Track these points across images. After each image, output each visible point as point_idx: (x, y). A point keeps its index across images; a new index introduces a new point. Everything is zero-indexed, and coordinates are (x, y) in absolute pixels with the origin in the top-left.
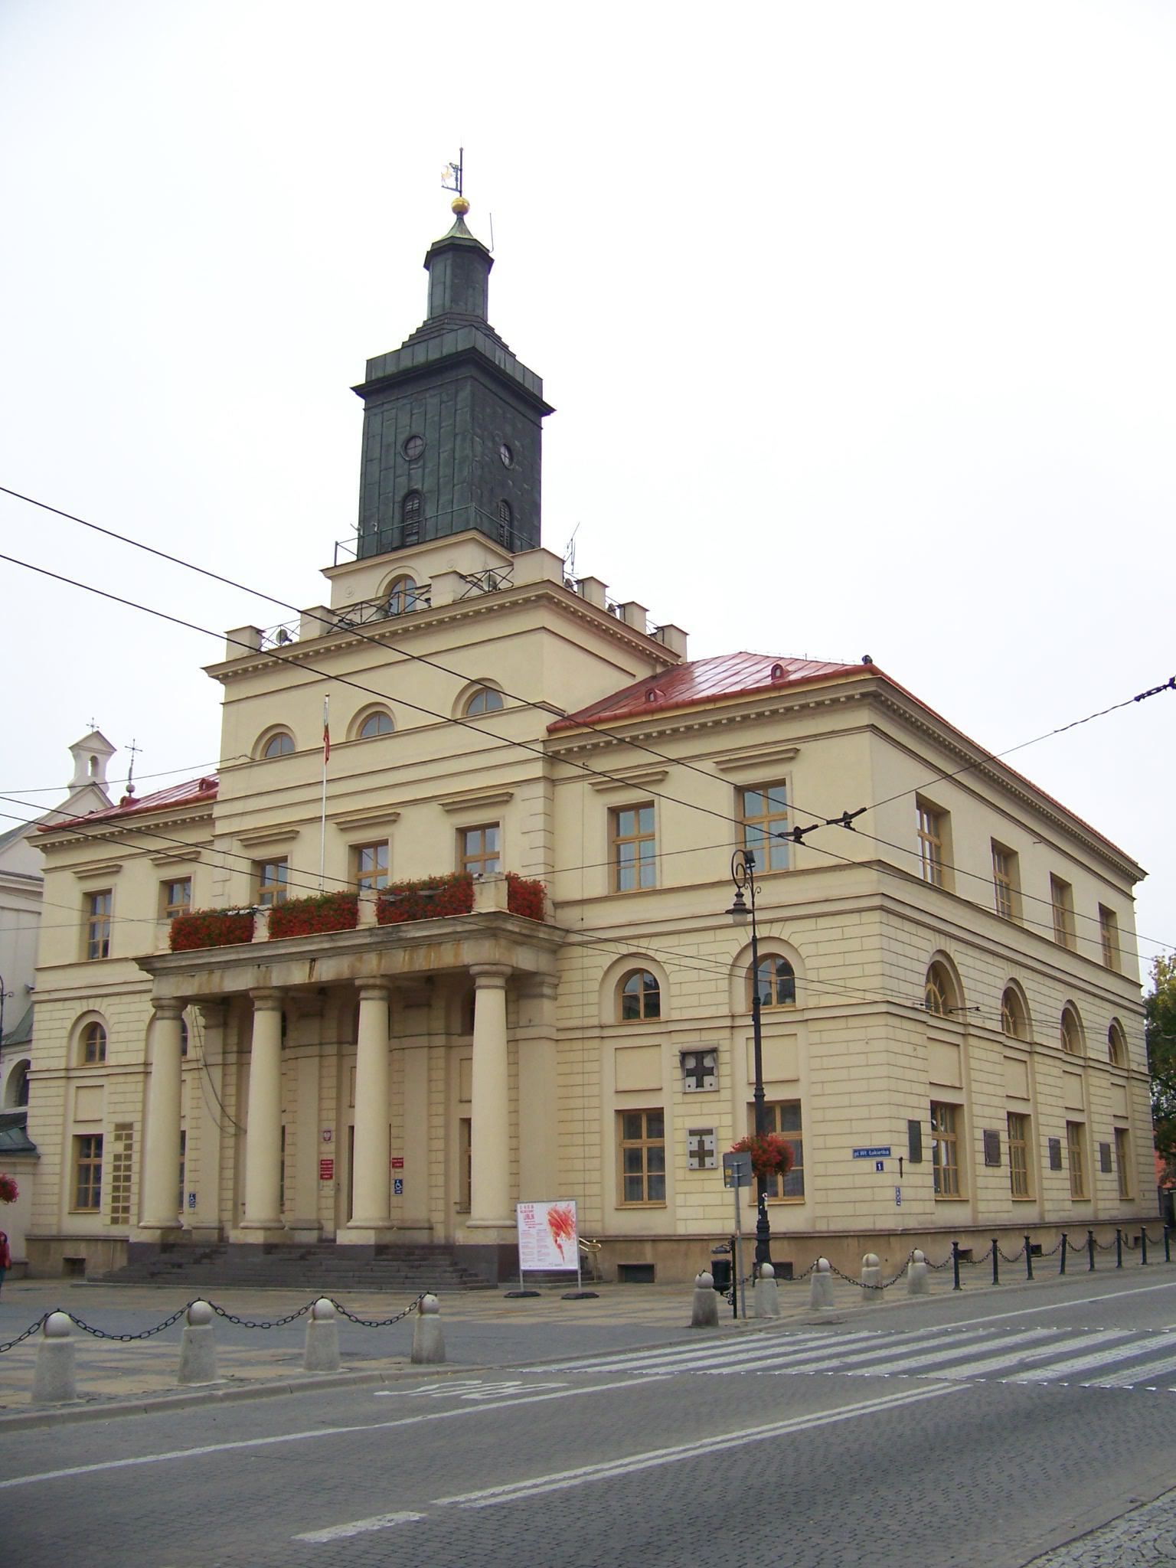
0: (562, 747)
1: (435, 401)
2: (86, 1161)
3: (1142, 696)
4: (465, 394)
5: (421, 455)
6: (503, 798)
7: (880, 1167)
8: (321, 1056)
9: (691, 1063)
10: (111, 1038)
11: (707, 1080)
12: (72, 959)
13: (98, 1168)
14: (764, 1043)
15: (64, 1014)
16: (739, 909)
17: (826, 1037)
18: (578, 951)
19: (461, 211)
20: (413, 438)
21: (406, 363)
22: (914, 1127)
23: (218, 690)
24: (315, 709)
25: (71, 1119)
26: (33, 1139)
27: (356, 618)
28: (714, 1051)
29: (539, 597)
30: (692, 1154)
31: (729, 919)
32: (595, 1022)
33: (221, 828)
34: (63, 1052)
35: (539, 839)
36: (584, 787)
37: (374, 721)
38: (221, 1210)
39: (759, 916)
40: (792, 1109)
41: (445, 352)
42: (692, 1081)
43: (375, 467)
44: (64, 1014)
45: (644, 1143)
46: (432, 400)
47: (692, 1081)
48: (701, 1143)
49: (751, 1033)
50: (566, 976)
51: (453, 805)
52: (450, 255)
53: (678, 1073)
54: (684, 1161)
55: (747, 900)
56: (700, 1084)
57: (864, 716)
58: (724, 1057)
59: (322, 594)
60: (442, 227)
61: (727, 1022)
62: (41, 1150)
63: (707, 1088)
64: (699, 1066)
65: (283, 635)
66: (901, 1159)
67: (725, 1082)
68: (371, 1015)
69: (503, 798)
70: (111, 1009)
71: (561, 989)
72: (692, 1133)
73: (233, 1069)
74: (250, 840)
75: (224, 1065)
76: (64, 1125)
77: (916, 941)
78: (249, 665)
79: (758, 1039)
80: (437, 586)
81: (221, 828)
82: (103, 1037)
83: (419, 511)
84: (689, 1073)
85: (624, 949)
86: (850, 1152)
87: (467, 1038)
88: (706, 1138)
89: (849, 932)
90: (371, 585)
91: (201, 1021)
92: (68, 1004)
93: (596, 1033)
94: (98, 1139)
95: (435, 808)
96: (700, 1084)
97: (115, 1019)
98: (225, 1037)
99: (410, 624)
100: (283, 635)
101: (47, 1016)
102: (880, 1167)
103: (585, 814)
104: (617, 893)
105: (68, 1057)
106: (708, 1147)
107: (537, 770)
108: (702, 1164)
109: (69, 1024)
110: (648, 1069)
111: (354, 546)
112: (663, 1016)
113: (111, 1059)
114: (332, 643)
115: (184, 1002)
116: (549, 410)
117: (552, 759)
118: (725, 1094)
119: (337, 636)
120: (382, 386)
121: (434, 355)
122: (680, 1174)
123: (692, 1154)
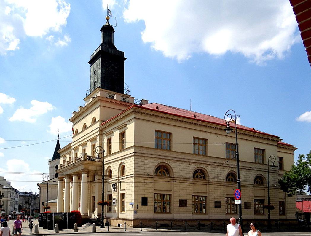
11: (115, 189)
28: (116, 184)
33: (72, 148)
57: (133, 116)
66: (138, 205)
81: (72, 148)
86: (129, 204)
88: (115, 200)
107: (98, 133)
116: (126, 59)
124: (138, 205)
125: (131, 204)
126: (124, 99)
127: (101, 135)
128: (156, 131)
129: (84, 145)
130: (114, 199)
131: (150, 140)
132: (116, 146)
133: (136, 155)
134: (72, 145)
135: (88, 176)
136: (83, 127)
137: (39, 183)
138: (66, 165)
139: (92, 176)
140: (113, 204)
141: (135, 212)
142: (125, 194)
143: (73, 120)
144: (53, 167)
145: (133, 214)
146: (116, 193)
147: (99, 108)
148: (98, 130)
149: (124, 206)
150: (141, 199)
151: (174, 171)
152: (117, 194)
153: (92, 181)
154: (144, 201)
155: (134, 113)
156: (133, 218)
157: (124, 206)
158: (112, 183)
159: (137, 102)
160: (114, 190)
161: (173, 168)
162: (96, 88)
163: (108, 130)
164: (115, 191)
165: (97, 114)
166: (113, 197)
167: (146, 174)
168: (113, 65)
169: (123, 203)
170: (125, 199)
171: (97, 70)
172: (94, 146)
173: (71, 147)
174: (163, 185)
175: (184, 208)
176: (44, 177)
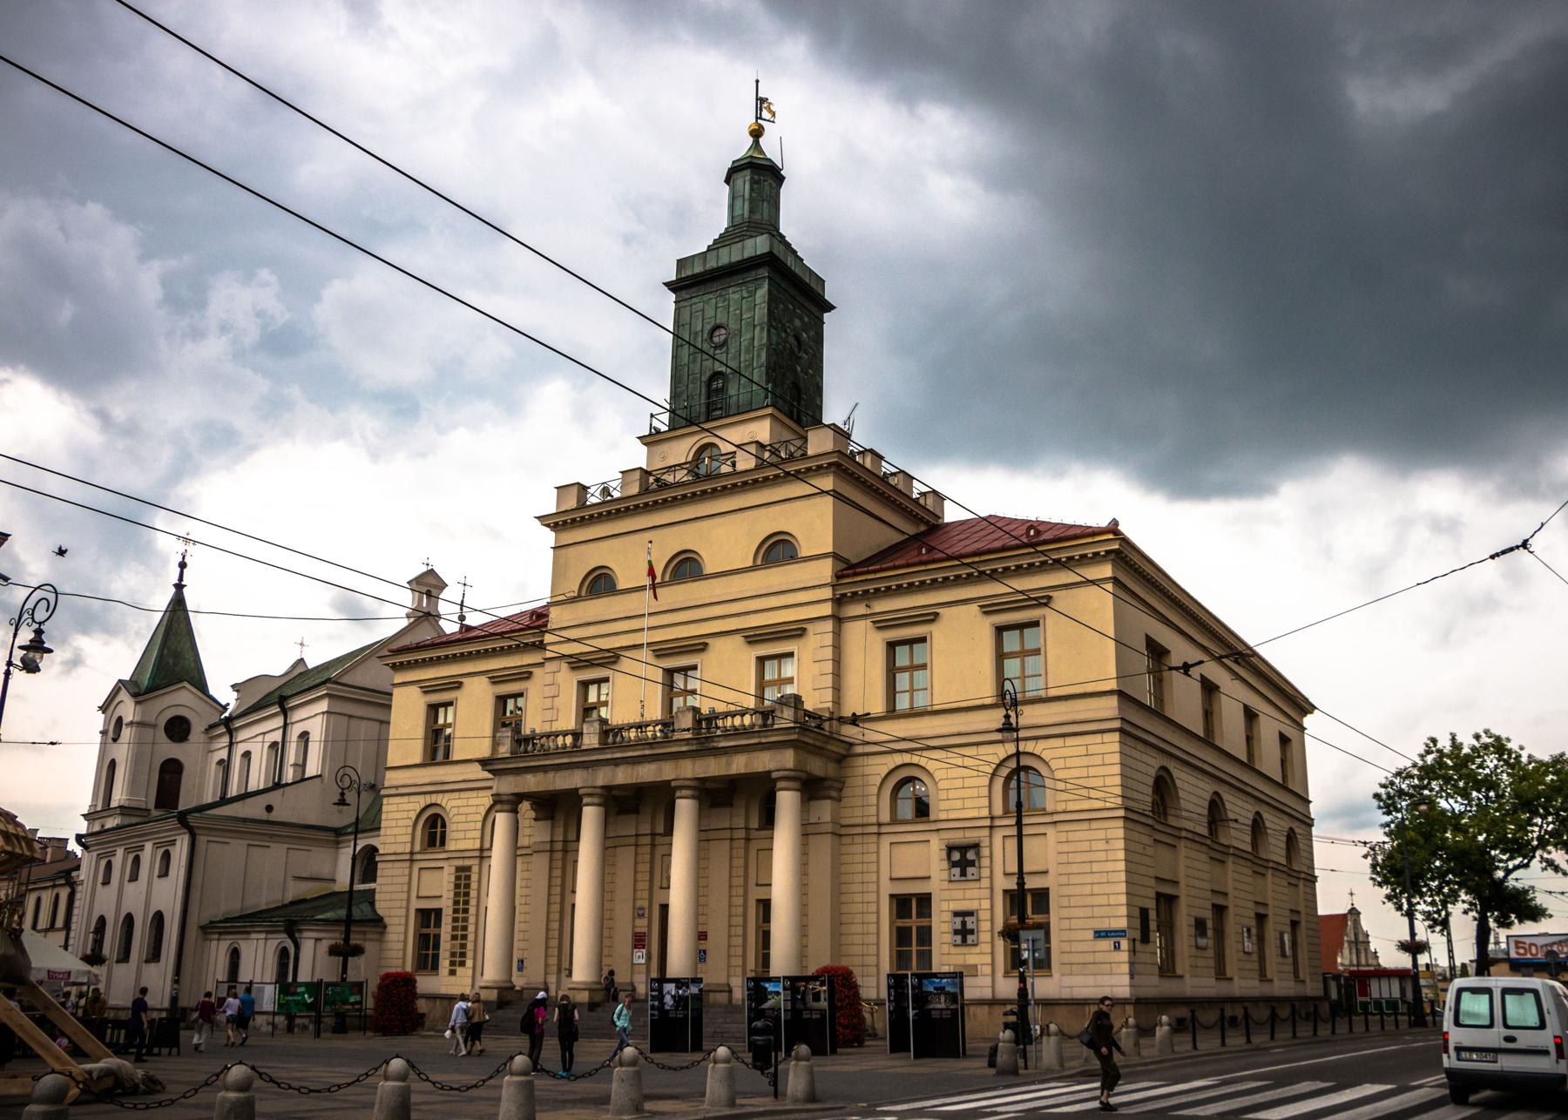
0: (848, 591)
1: (737, 296)
2: (425, 931)
3: (1498, 555)
4: (762, 293)
5: (725, 343)
6: (797, 631)
7: (1117, 947)
8: (637, 845)
9: (956, 856)
10: (451, 827)
11: (970, 870)
12: (418, 760)
13: (437, 937)
14: (1025, 840)
15: (410, 806)
16: (1008, 727)
17: (1071, 836)
18: (860, 761)
19: (757, 133)
20: (717, 327)
21: (712, 264)
22: (1144, 913)
23: (549, 537)
24: (629, 556)
25: (414, 894)
26: (380, 912)
27: (669, 478)
28: (976, 846)
29: (830, 465)
30: (956, 932)
31: (999, 736)
32: (874, 820)
34: (409, 838)
35: (829, 667)
36: (865, 625)
37: (686, 567)
38: (546, 973)
39: (1022, 734)
40: (1042, 896)
41: (746, 255)
42: (957, 871)
43: (685, 351)
44: (410, 806)
45: (914, 922)
46: (734, 295)
47: (957, 871)
48: (964, 923)
49: (1014, 831)
50: (849, 782)
51: (754, 637)
52: (748, 172)
53: (945, 865)
54: (948, 938)
55: (1013, 720)
56: (963, 874)
58: (985, 852)
59: (638, 457)
61: (987, 823)
62: (387, 920)
63: (969, 877)
64: (963, 858)
65: (606, 491)
67: (985, 872)
68: (685, 810)
69: (797, 631)
70: (451, 804)
71: (845, 792)
72: (956, 914)
73: (559, 855)
74: (577, 663)
75: (551, 851)
76: (408, 900)
77: (1145, 758)
78: (575, 515)
79: (1020, 836)
80: (740, 455)
82: (444, 825)
83: (722, 390)
84: (954, 864)
85: (899, 759)
86: (1091, 935)
87: (764, 833)
89: (1092, 749)
90: (681, 451)
91: (533, 814)
92: (413, 798)
93: (875, 829)
94: (438, 912)
95: (738, 640)
96: (963, 874)
97: (455, 811)
98: (553, 827)
99: (719, 484)
100: (606, 491)
101: (394, 808)
102: (1117, 947)
103: (866, 647)
104: (892, 713)
105: (413, 842)
106: (969, 926)
107: (827, 609)
108: (964, 941)
109: (413, 815)
110: (919, 859)
111: (665, 418)
112: (932, 817)
113: (450, 846)
114: (650, 499)
115: (519, 797)
116: (830, 308)
117: (839, 601)
118: (985, 883)
119: (650, 495)
120: (691, 282)
121: (736, 258)
122: (946, 949)
123: (956, 932)
127: (838, 620)
144: (155, 726)
148: (827, 593)
168: (797, 323)
171: (733, 326)
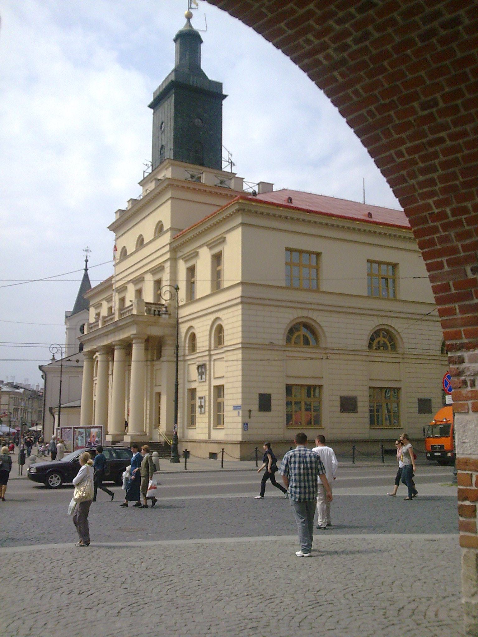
6: (160, 269)
11: (204, 376)
19: (189, 17)
57: (239, 220)
58: (208, 367)
60: (180, 25)
86: (232, 408)
88: (203, 400)
107: (168, 256)
116: (225, 96)
124: (250, 411)
125: (236, 408)
126: (222, 182)
127: (174, 260)
128: (287, 249)
129: (139, 280)
130: (201, 398)
131: (276, 270)
132: (203, 285)
133: (246, 303)
134: (113, 281)
135: (146, 349)
136: (138, 241)
137: (45, 364)
138: (100, 326)
139: (155, 347)
140: (198, 410)
141: (245, 426)
142: (223, 386)
143: (115, 228)
145: (240, 431)
146: (204, 384)
147: (170, 201)
148: (167, 248)
149: (222, 413)
150: (257, 397)
151: (327, 335)
152: (207, 388)
153: (155, 359)
154: (265, 402)
155: (240, 212)
156: (240, 439)
157: (222, 413)
158: (198, 363)
159: (250, 186)
160: (201, 379)
161: (325, 329)
162: (165, 160)
163: (188, 249)
164: (204, 380)
165: (164, 213)
166: (199, 394)
167: (267, 342)
169: (219, 407)
170: (224, 397)
172: (158, 283)
173: (112, 285)
174: (303, 367)
175: (352, 415)
176: (55, 350)
